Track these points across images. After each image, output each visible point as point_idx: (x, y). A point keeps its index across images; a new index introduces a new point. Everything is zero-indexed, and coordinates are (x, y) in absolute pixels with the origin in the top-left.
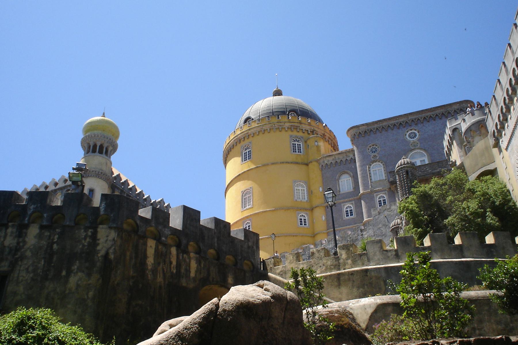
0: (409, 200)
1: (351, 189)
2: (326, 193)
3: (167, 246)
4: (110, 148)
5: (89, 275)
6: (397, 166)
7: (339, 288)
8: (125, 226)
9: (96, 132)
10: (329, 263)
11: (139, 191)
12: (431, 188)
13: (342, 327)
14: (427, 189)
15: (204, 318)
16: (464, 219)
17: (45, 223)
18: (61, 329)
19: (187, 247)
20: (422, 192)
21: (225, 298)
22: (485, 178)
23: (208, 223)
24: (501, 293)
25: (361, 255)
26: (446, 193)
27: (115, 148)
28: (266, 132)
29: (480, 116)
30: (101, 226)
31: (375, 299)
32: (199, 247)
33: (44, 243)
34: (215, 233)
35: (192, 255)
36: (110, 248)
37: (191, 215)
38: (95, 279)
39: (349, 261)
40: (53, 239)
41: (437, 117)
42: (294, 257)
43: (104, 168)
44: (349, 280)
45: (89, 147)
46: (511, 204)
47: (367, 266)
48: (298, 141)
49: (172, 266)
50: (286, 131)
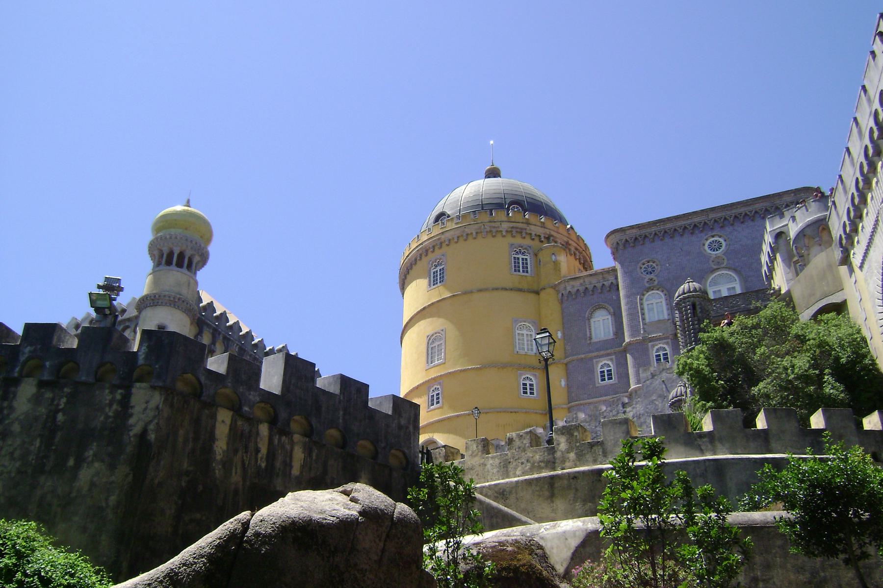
0: (695, 353)
1: (611, 336)
2: (538, 336)
3: (252, 421)
4: (196, 259)
5: (112, 467)
6: (677, 295)
7: (553, 502)
8: (180, 386)
9: (173, 231)
10: (537, 457)
11: (245, 330)
12: (732, 334)
13: (516, 570)
14: (725, 335)
15: (218, 546)
16: (787, 386)
17: (46, 377)
18: (50, 558)
19: (289, 424)
20: (716, 339)
21: (265, 512)
22: (826, 317)
23: (330, 384)
24: (791, 515)
25: (591, 445)
26: (759, 341)
27: (204, 259)
28: (470, 237)
29: (819, 211)
30: (138, 385)
31: (584, 522)
32: (311, 425)
33: (42, 410)
34: (340, 402)
35: (297, 437)
36: (151, 421)
37: (299, 370)
38: (122, 473)
39: (572, 455)
40: (58, 405)
41: (757, 215)
42: (480, 447)
43: (184, 291)
44: (569, 487)
45: (161, 256)
46: (867, 361)
47: (601, 464)
48: (523, 254)
49: (260, 455)
50: (504, 236)
